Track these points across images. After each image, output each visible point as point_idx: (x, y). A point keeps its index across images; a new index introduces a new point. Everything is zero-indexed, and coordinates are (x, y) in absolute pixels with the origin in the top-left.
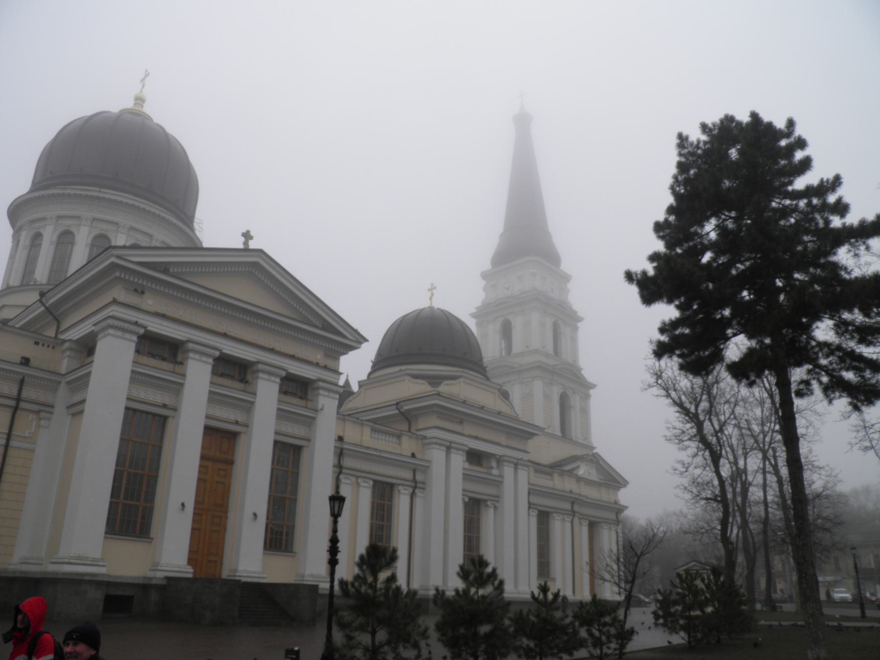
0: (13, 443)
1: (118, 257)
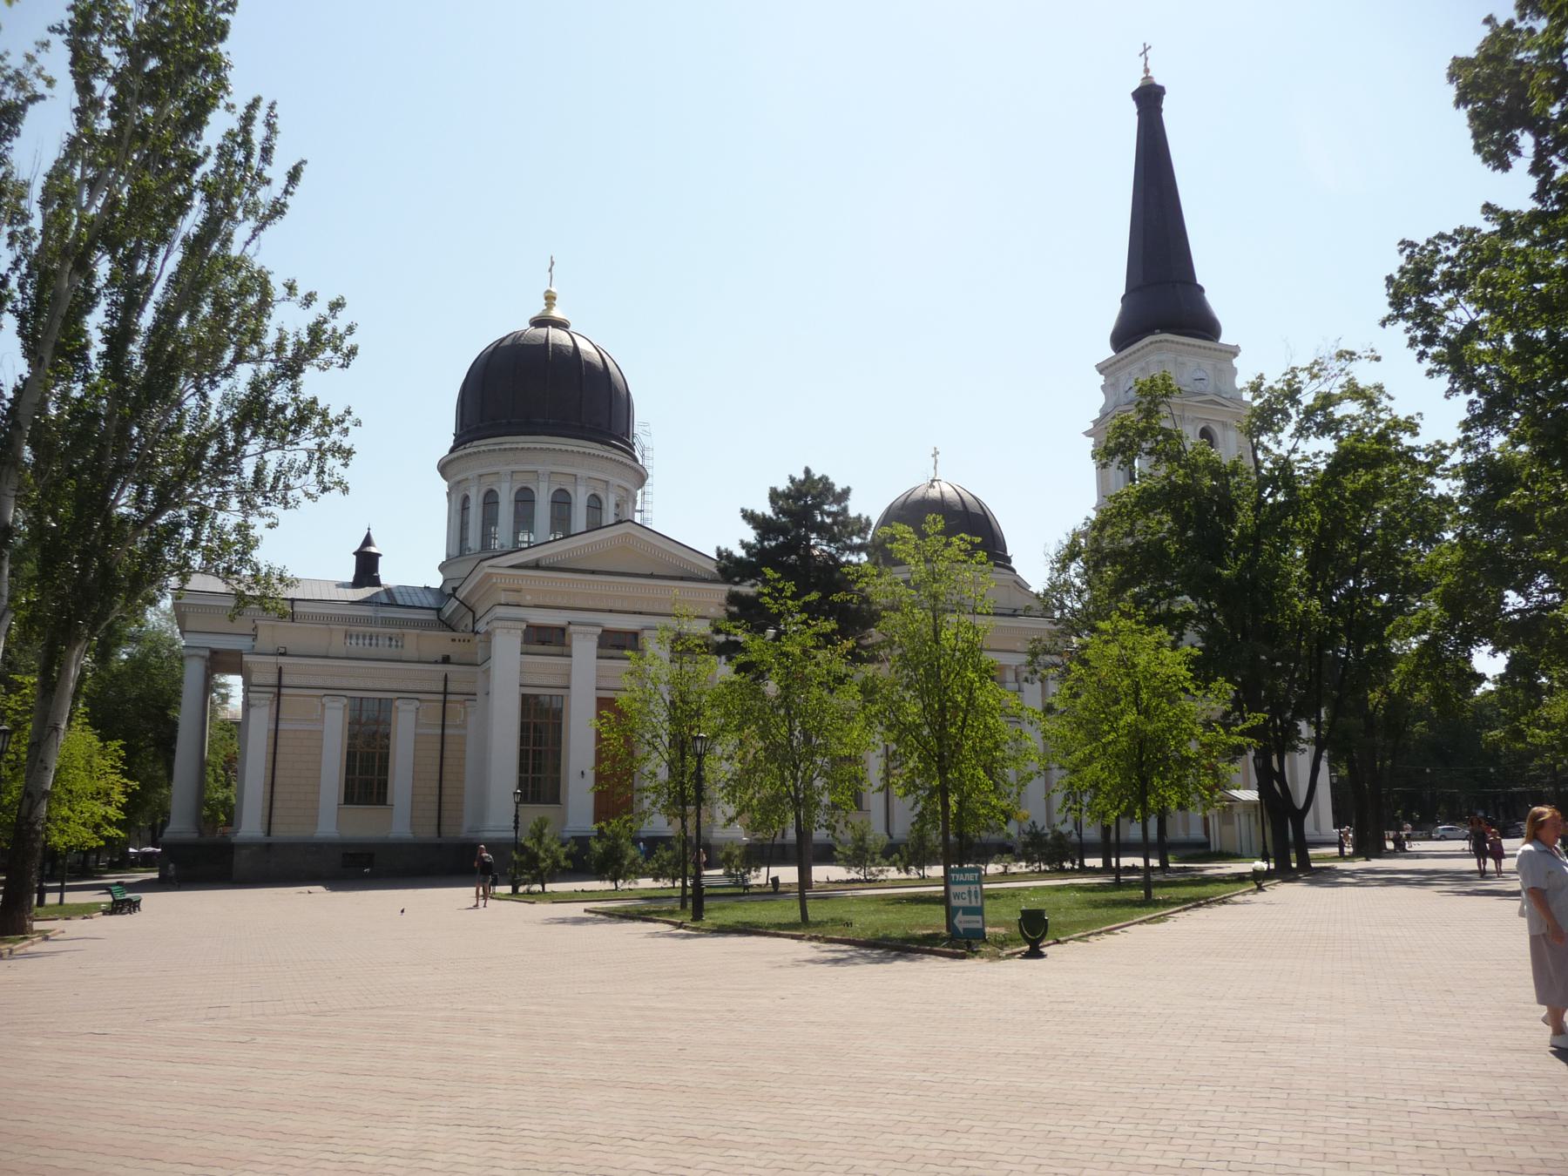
0: (447, 731)
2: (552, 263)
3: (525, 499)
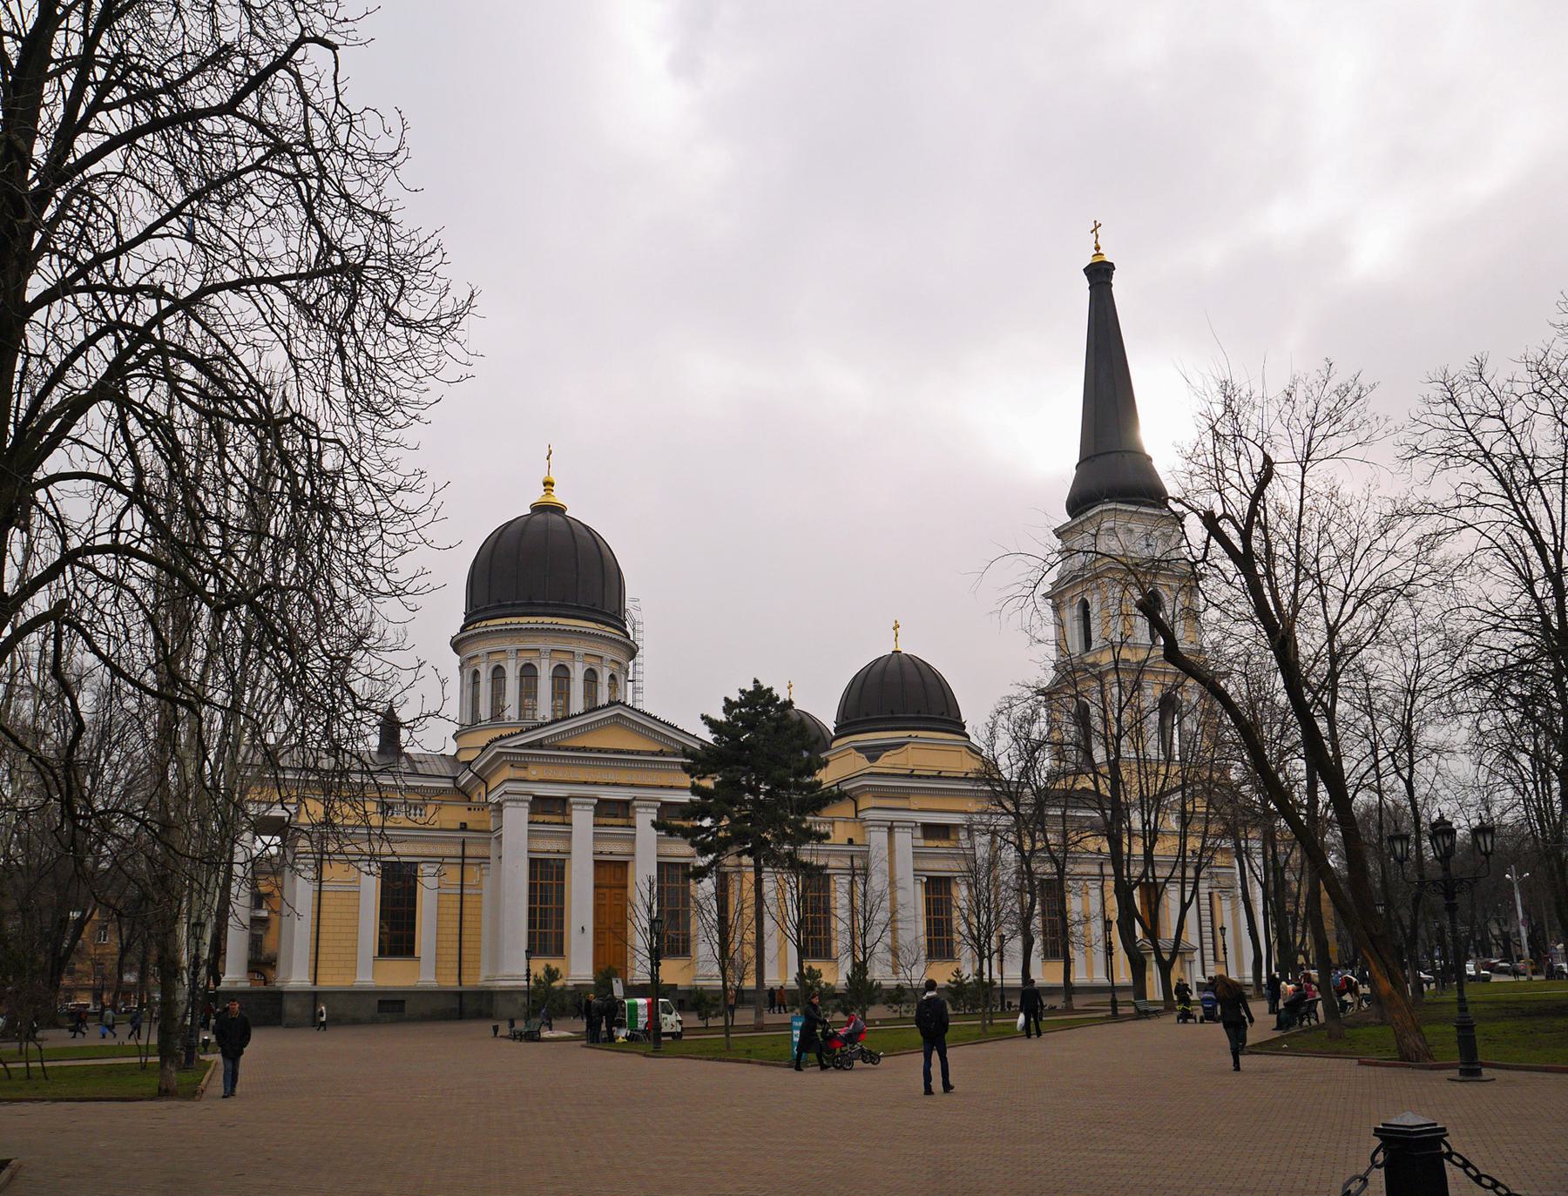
0: (465, 891)
1: (500, 747)
2: (550, 452)
3: (528, 674)
